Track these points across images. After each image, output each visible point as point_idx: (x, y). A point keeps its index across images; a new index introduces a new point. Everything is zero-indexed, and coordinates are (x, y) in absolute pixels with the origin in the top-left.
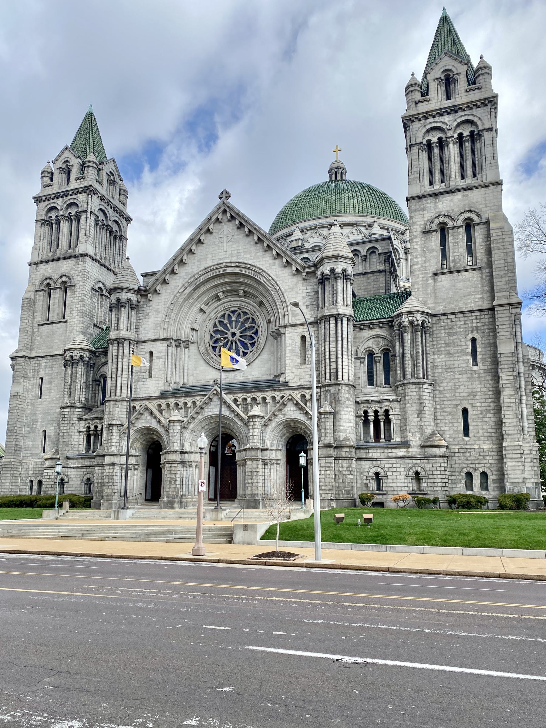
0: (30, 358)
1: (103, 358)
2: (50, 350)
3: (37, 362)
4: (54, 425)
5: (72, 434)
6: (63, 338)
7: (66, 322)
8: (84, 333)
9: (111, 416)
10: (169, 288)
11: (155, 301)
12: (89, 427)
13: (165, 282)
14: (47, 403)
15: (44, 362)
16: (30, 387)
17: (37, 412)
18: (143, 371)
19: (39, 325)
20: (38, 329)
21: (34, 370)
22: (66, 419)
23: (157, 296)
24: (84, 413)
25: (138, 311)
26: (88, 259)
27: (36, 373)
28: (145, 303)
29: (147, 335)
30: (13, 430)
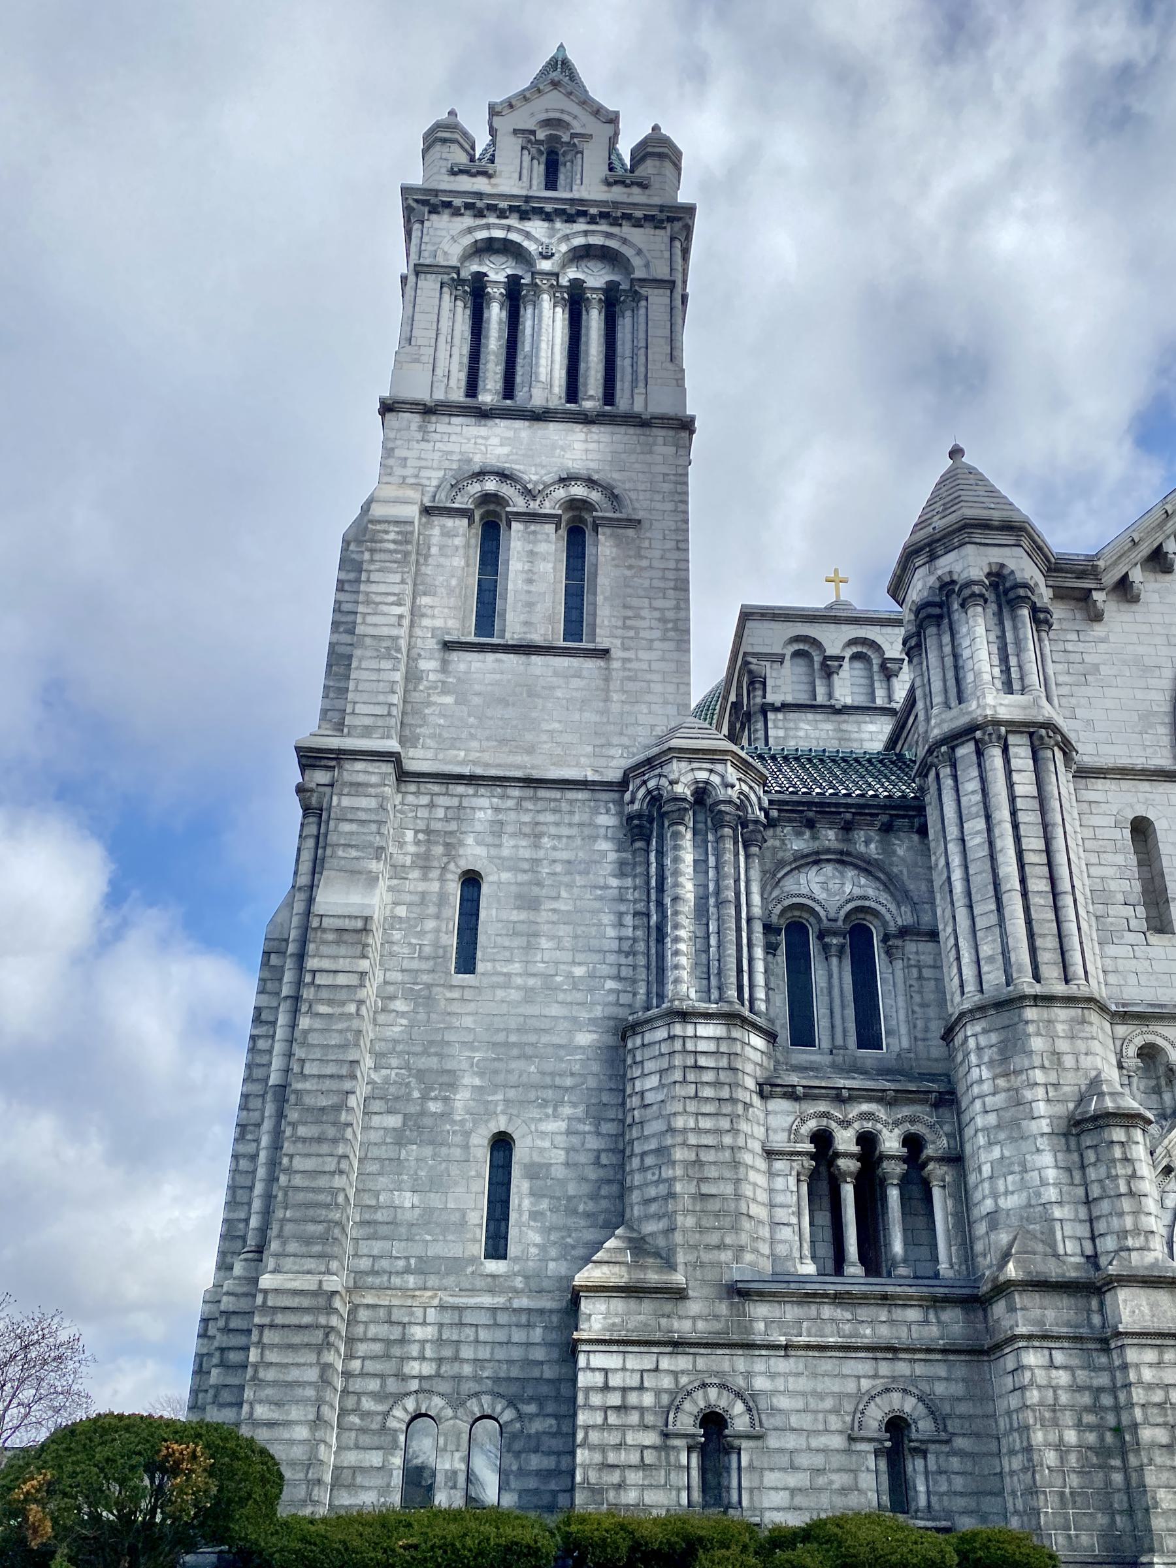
2: (518, 759)
4: (567, 1110)
6: (590, 716)
12: (822, 1139)
16: (401, 911)
17: (450, 1037)
21: (428, 832)
22: (709, 1077)
27: (439, 850)
30: (337, 1108)
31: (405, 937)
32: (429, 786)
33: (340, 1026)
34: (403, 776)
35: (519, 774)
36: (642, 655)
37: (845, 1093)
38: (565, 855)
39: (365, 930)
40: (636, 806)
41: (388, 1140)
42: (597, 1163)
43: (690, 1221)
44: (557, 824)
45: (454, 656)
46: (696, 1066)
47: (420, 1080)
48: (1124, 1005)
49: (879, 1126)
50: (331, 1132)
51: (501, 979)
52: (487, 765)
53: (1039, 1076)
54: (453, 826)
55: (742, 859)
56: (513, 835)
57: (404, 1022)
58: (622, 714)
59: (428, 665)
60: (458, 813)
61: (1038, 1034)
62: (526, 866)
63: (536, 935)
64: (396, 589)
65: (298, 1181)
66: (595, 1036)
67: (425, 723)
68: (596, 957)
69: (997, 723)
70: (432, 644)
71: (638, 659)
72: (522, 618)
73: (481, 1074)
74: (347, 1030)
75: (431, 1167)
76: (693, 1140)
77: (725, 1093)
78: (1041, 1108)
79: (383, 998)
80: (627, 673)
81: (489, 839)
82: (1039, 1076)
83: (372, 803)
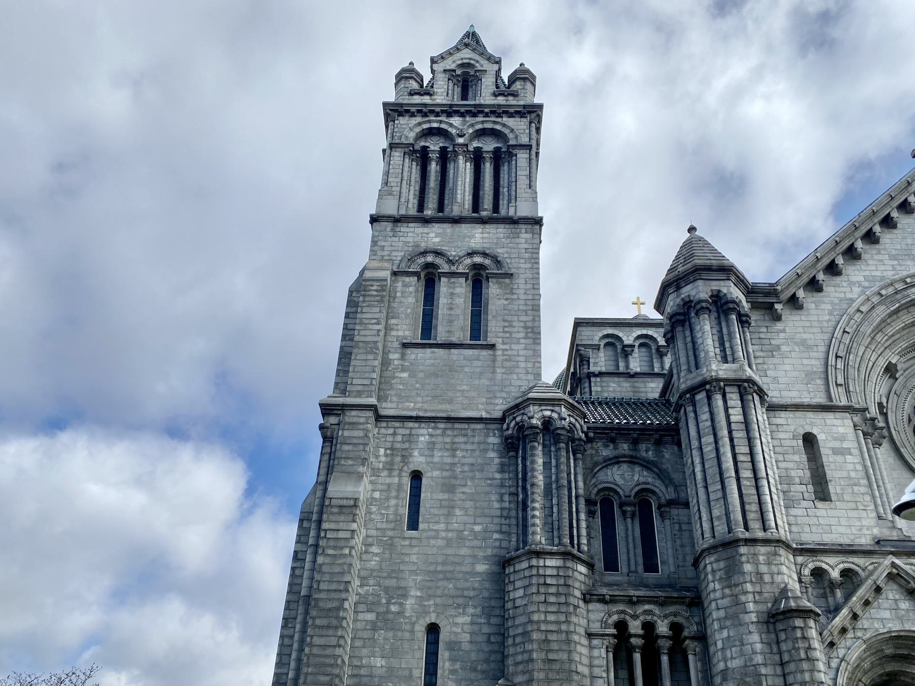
2: (444, 407)
6: (485, 382)
9: (767, 588)
12: (622, 626)
16: (377, 495)
21: (392, 449)
22: (553, 590)
27: (398, 459)
31: (378, 509)
33: (340, 562)
34: (379, 418)
35: (444, 415)
36: (514, 347)
37: (635, 599)
38: (470, 460)
39: (356, 506)
40: (510, 432)
41: (368, 627)
42: (489, 641)
43: (542, 675)
44: (466, 443)
45: (409, 351)
46: (545, 584)
47: (386, 593)
48: (801, 544)
49: (655, 618)
50: (334, 622)
51: (433, 533)
52: (426, 411)
53: (749, 587)
54: (407, 445)
55: (572, 461)
56: (441, 449)
57: (377, 559)
58: (502, 380)
59: (394, 356)
60: (410, 438)
61: (748, 562)
62: (448, 467)
63: (453, 507)
64: (377, 316)
65: (315, 651)
66: (487, 567)
67: (392, 388)
68: (488, 520)
69: (718, 380)
70: (396, 344)
71: (511, 349)
72: (447, 329)
73: (420, 589)
74: (344, 563)
75: (393, 644)
76: (543, 628)
77: (562, 600)
78: (751, 606)
79: (365, 545)
80: (505, 357)
81: (427, 453)
82: (749, 587)
83: (361, 433)
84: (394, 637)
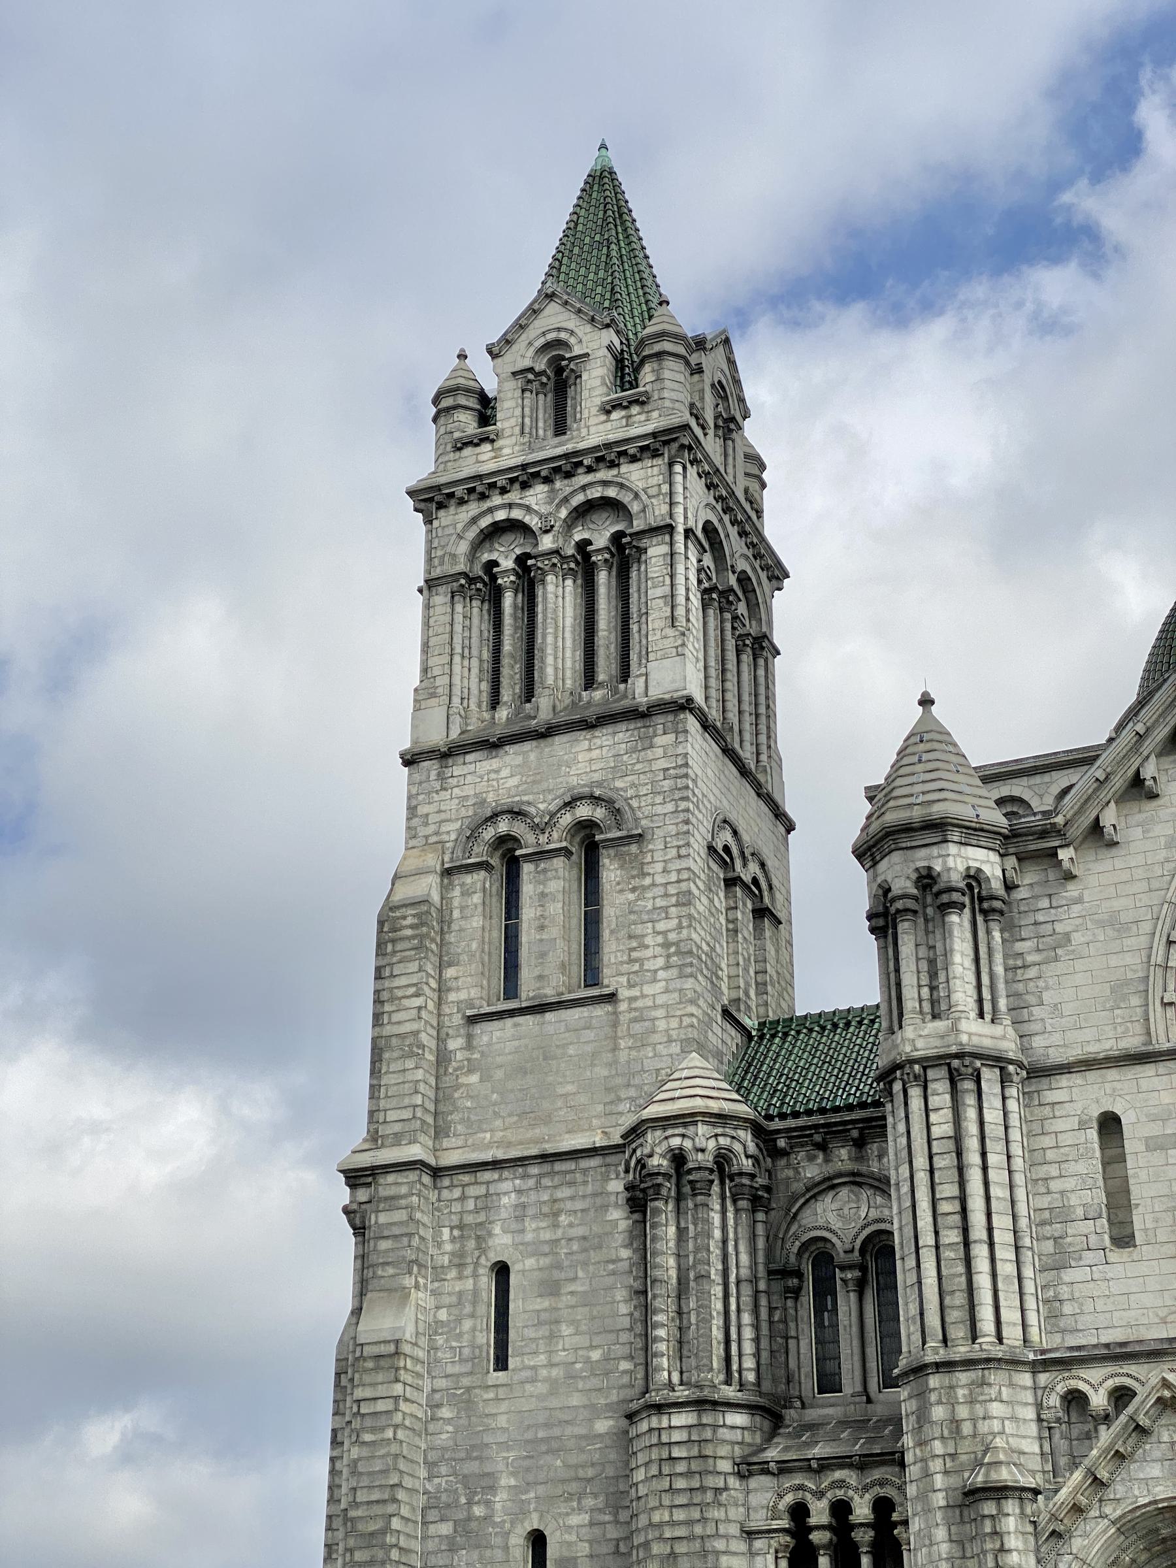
0: (437, 1172)
1: (811, 1159)
3: (472, 1191)
5: (720, 1545)
7: (611, 998)
8: (701, 1048)
9: (965, 1446)
10: (1164, 814)
11: (1092, 880)
12: (799, 1512)
13: (1138, 789)
14: (541, 1388)
15: (508, 1190)
16: (443, 1315)
17: (488, 1439)
18: (1080, 1212)
19: (473, 1020)
20: (469, 1037)
21: (461, 1227)
22: (681, 1467)
23: (1104, 853)
24: (758, 1440)
25: (1010, 928)
26: (692, 723)
27: (471, 1244)
28: (1038, 890)
29: (1071, 1036)
31: (447, 1340)
32: (461, 1177)
33: (382, 1452)
37: (814, 1464)
38: (579, 1231)
41: (443, 1548)
42: (617, 1552)
44: (572, 1198)
46: (671, 1458)
47: (466, 1487)
48: (1043, 1352)
49: (851, 1493)
50: (380, 1554)
54: (481, 1218)
57: (450, 1429)
58: (628, 1062)
61: (939, 1402)
62: (546, 1249)
66: (611, 1423)
71: (643, 996)
73: (513, 1474)
74: (388, 1454)
79: (431, 1407)
80: (634, 1014)
83: (401, 1215)
84: (481, 1557)
